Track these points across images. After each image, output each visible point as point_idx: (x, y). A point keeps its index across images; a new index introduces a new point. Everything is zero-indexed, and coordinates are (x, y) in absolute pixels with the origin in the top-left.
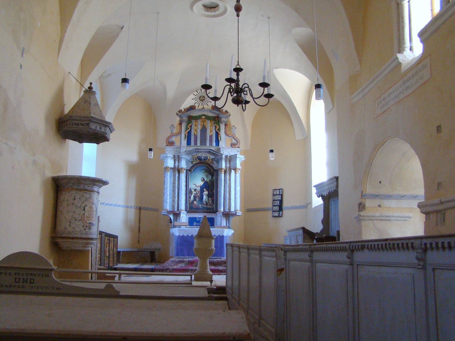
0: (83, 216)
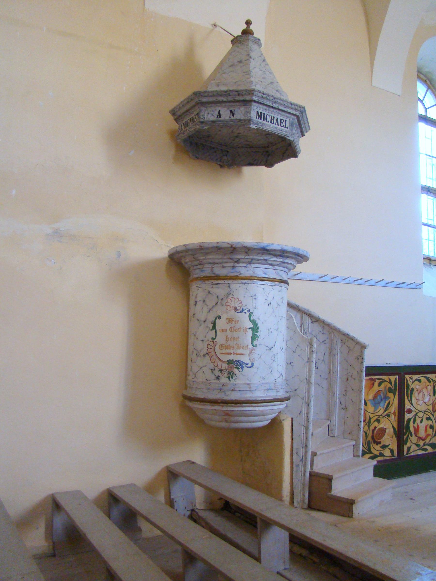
0: (211, 343)
